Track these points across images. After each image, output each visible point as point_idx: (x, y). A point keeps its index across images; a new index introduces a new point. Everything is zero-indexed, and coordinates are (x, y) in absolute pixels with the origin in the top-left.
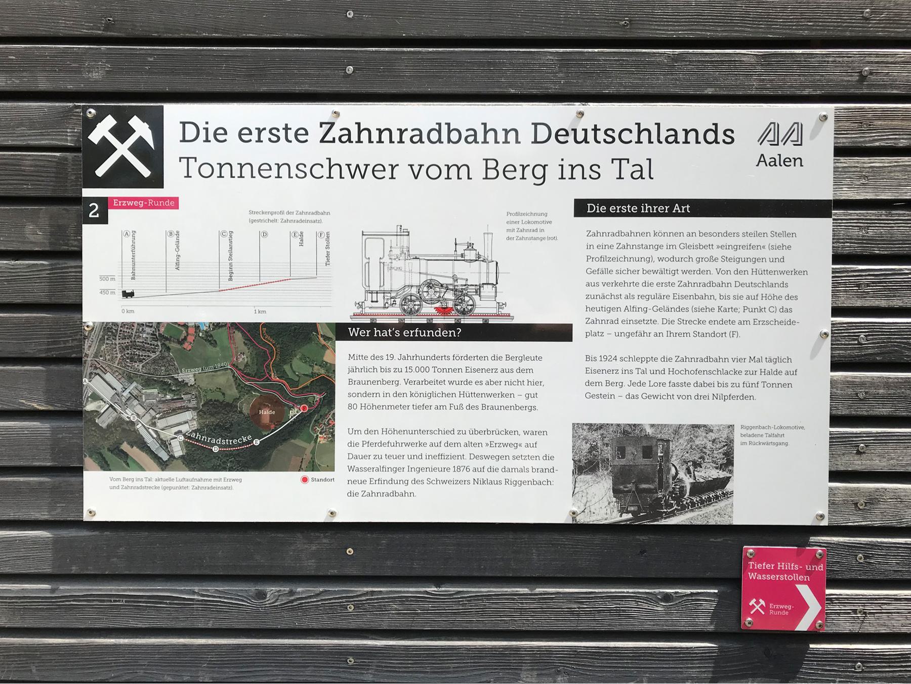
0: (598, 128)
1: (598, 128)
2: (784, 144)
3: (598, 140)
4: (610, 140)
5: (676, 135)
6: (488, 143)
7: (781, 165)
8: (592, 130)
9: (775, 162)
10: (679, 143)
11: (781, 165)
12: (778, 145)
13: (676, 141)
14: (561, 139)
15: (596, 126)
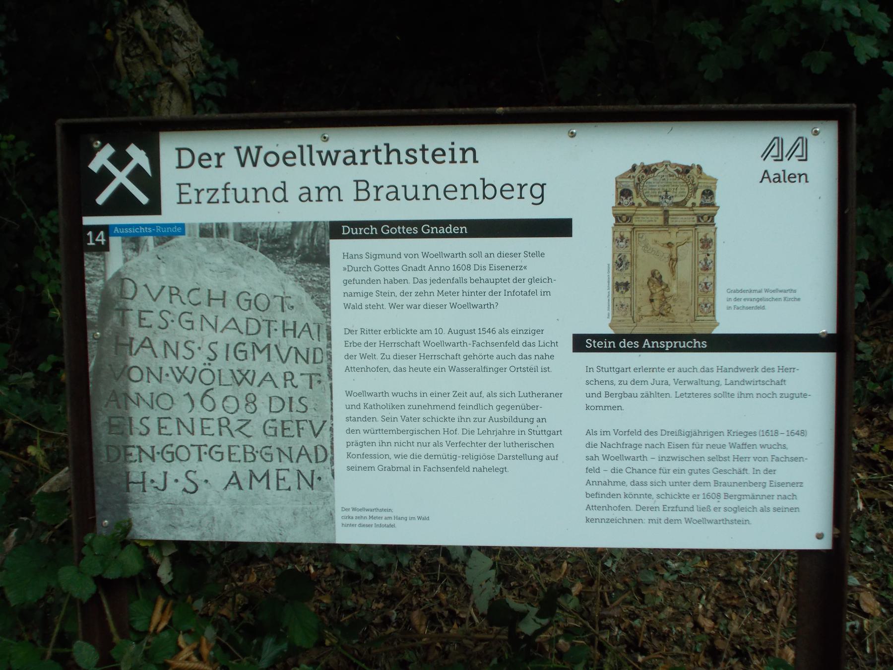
0: (426, 148)
1: (426, 148)
2: (789, 159)
3: (380, 160)
4: (411, 160)
5: (354, 157)
6: (391, 163)
7: (785, 182)
8: (380, 150)
9: (779, 177)
10: (357, 164)
11: (785, 182)
12: (782, 160)
13: (354, 163)
14: (438, 158)
15: (423, 146)
